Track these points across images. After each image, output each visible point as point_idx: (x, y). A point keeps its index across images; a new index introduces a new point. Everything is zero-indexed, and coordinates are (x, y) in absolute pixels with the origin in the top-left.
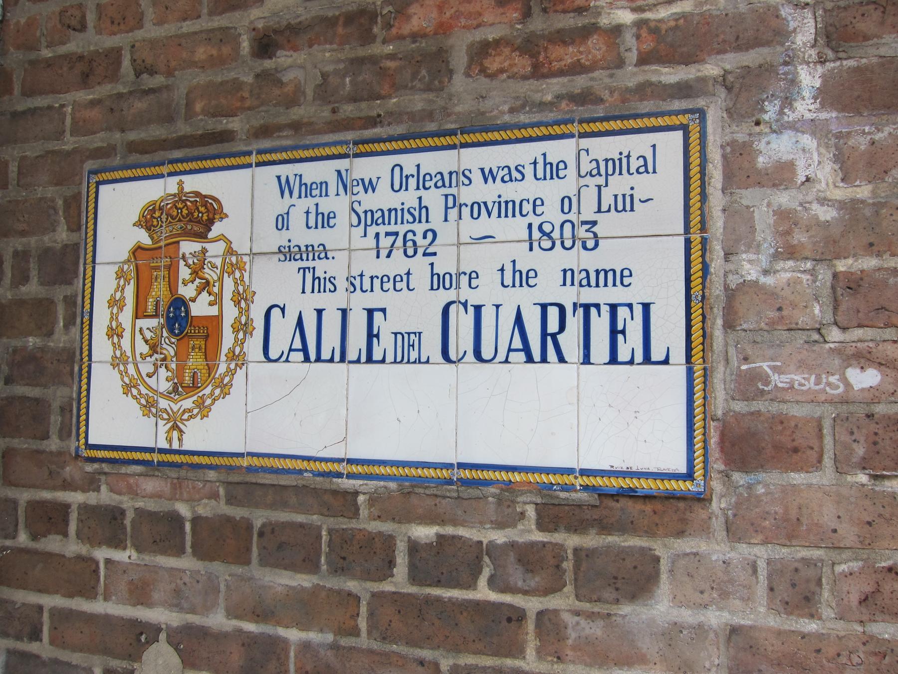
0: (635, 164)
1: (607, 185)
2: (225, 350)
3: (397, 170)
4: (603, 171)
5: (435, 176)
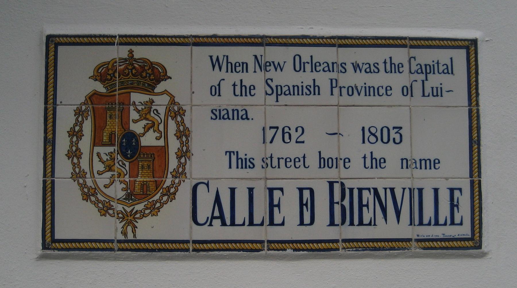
0: (441, 68)
1: (427, 80)
2: (171, 169)
3: (297, 58)
5: (323, 64)
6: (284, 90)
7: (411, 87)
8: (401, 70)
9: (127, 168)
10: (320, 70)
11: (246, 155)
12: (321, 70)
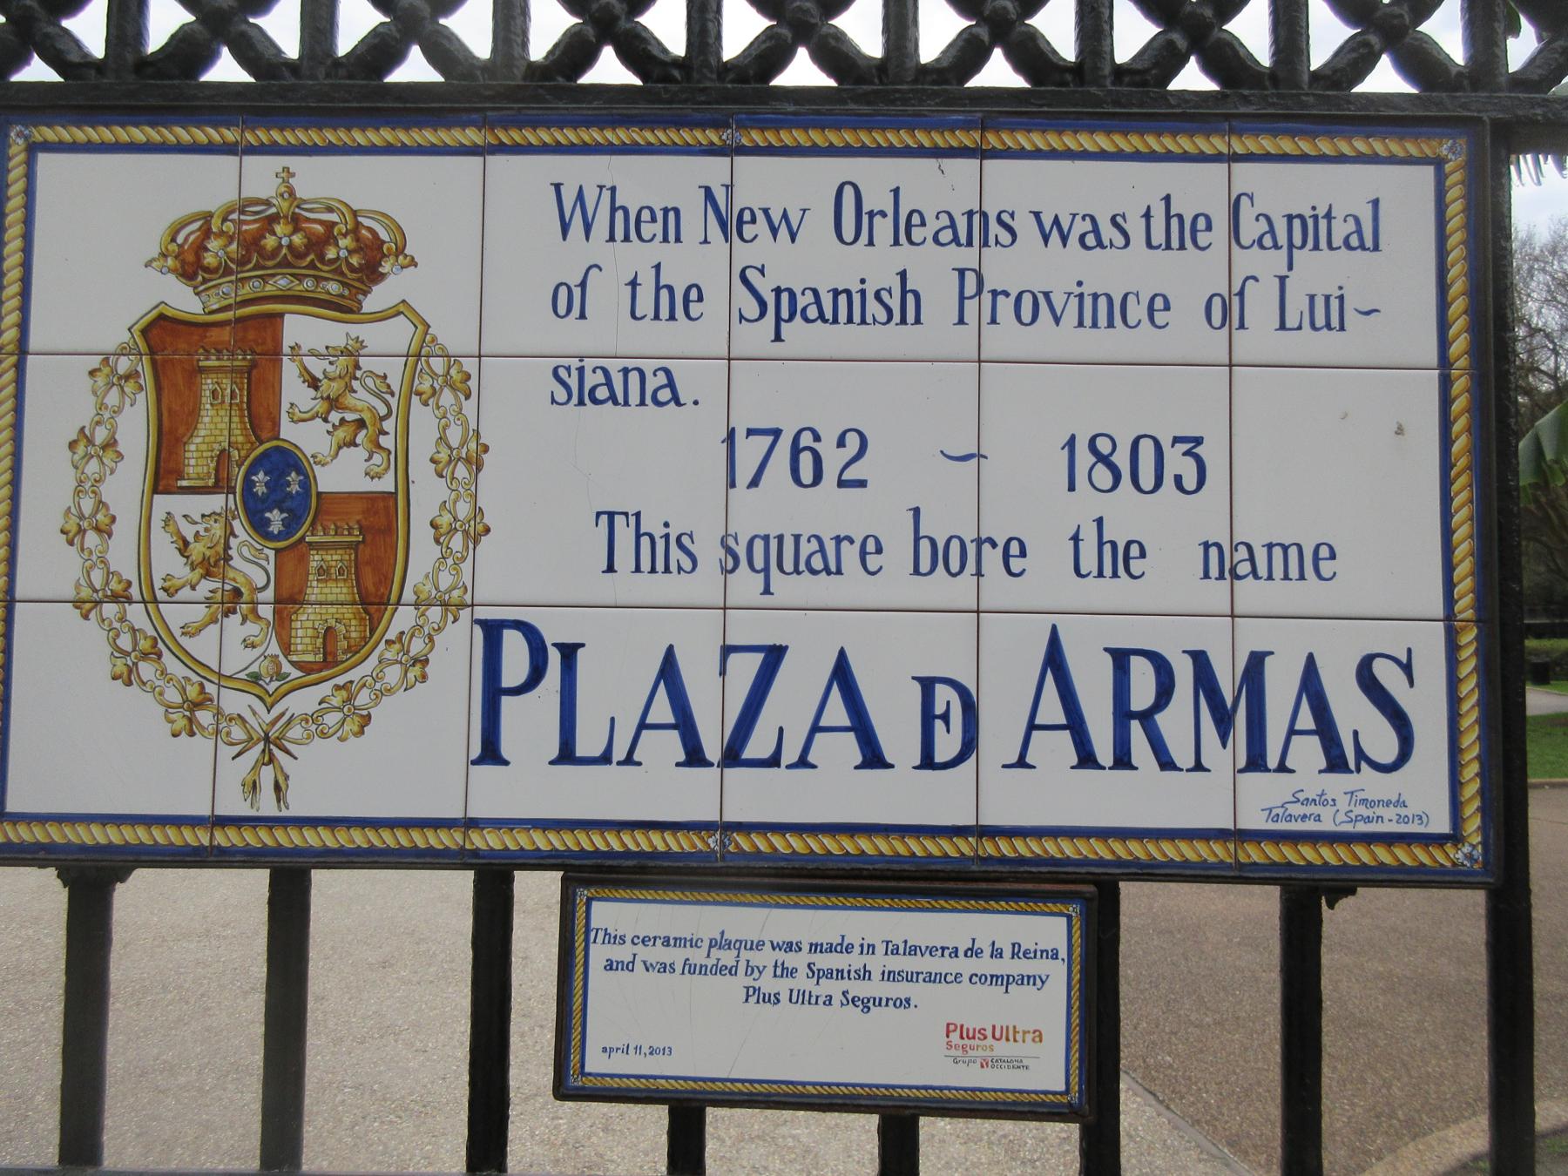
1: (1290, 268)
3: (849, 195)
4: (1282, 239)
7: (1241, 294)
8: (1203, 239)
11: (666, 525)
12: (930, 240)
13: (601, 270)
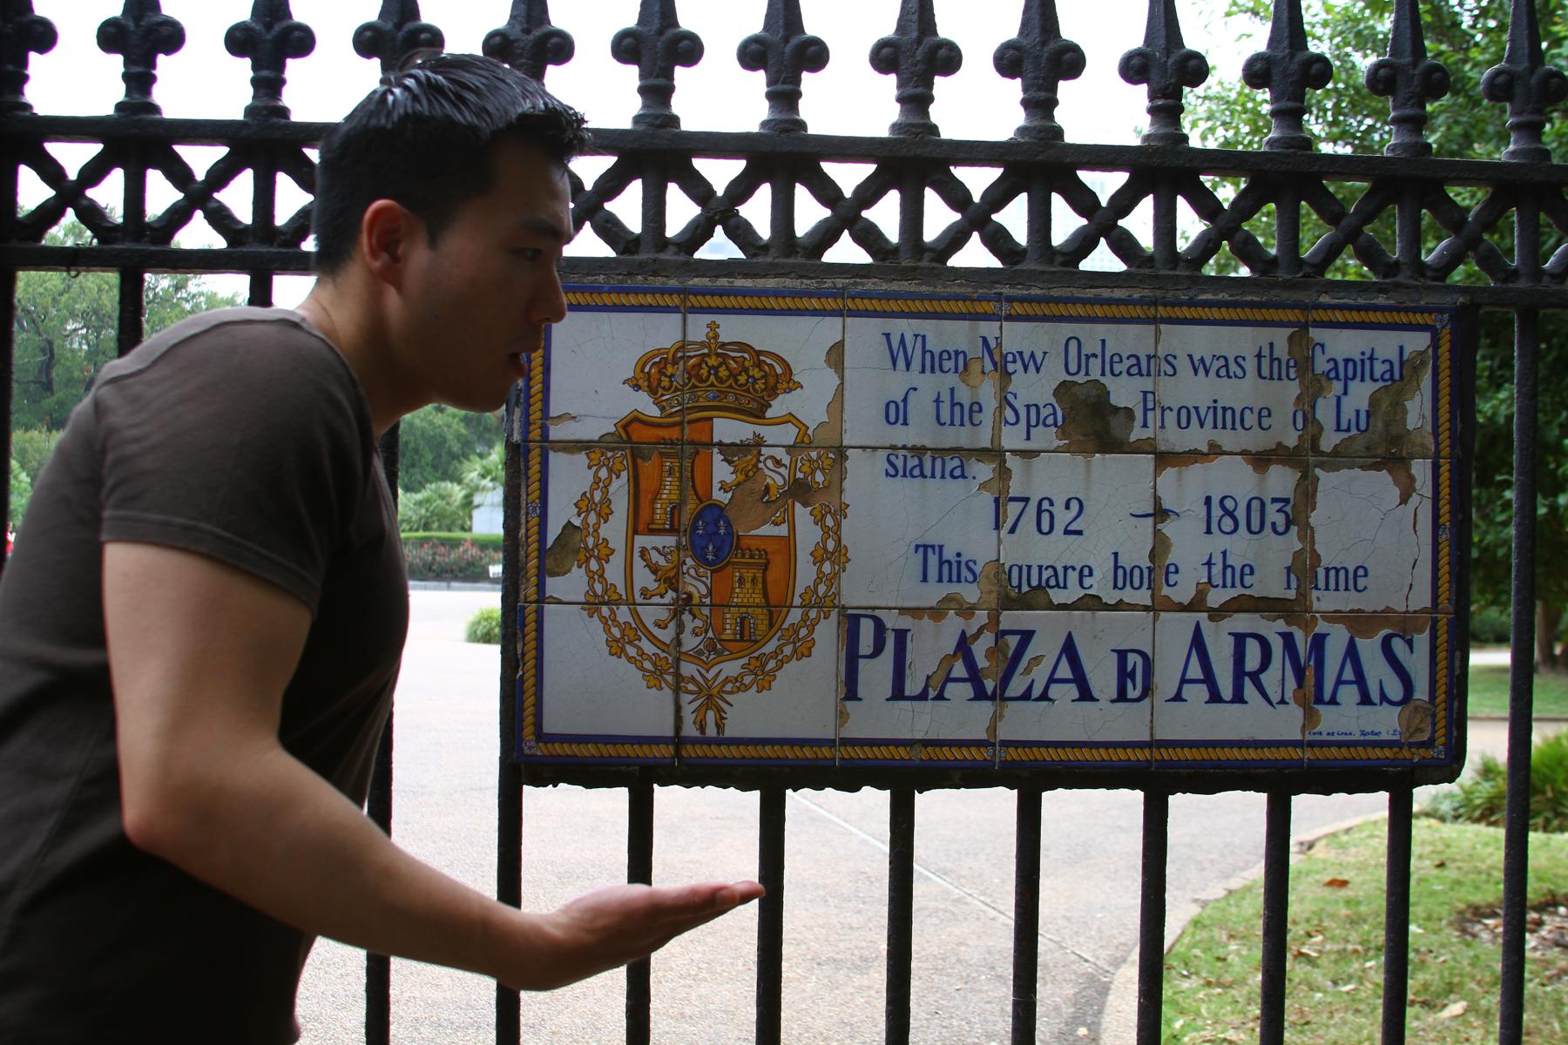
0: (1379, 369)
1: (1345, 393)
2: (799, 589)
3: (1073, 345)
4: (1342, 375)
5: (1128, 358)
6: (1042, 417)
9: (708, 582)
10: (1121, 372)
11: (959, 555)
13: (915, 389)
